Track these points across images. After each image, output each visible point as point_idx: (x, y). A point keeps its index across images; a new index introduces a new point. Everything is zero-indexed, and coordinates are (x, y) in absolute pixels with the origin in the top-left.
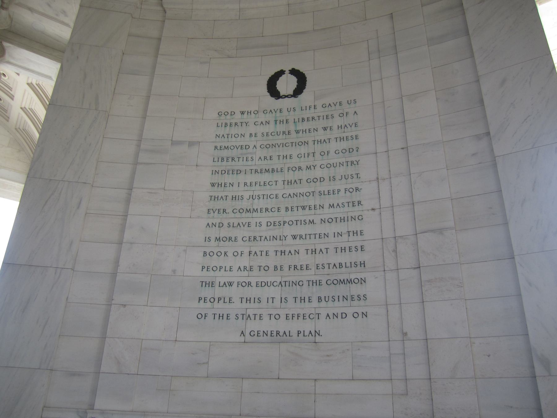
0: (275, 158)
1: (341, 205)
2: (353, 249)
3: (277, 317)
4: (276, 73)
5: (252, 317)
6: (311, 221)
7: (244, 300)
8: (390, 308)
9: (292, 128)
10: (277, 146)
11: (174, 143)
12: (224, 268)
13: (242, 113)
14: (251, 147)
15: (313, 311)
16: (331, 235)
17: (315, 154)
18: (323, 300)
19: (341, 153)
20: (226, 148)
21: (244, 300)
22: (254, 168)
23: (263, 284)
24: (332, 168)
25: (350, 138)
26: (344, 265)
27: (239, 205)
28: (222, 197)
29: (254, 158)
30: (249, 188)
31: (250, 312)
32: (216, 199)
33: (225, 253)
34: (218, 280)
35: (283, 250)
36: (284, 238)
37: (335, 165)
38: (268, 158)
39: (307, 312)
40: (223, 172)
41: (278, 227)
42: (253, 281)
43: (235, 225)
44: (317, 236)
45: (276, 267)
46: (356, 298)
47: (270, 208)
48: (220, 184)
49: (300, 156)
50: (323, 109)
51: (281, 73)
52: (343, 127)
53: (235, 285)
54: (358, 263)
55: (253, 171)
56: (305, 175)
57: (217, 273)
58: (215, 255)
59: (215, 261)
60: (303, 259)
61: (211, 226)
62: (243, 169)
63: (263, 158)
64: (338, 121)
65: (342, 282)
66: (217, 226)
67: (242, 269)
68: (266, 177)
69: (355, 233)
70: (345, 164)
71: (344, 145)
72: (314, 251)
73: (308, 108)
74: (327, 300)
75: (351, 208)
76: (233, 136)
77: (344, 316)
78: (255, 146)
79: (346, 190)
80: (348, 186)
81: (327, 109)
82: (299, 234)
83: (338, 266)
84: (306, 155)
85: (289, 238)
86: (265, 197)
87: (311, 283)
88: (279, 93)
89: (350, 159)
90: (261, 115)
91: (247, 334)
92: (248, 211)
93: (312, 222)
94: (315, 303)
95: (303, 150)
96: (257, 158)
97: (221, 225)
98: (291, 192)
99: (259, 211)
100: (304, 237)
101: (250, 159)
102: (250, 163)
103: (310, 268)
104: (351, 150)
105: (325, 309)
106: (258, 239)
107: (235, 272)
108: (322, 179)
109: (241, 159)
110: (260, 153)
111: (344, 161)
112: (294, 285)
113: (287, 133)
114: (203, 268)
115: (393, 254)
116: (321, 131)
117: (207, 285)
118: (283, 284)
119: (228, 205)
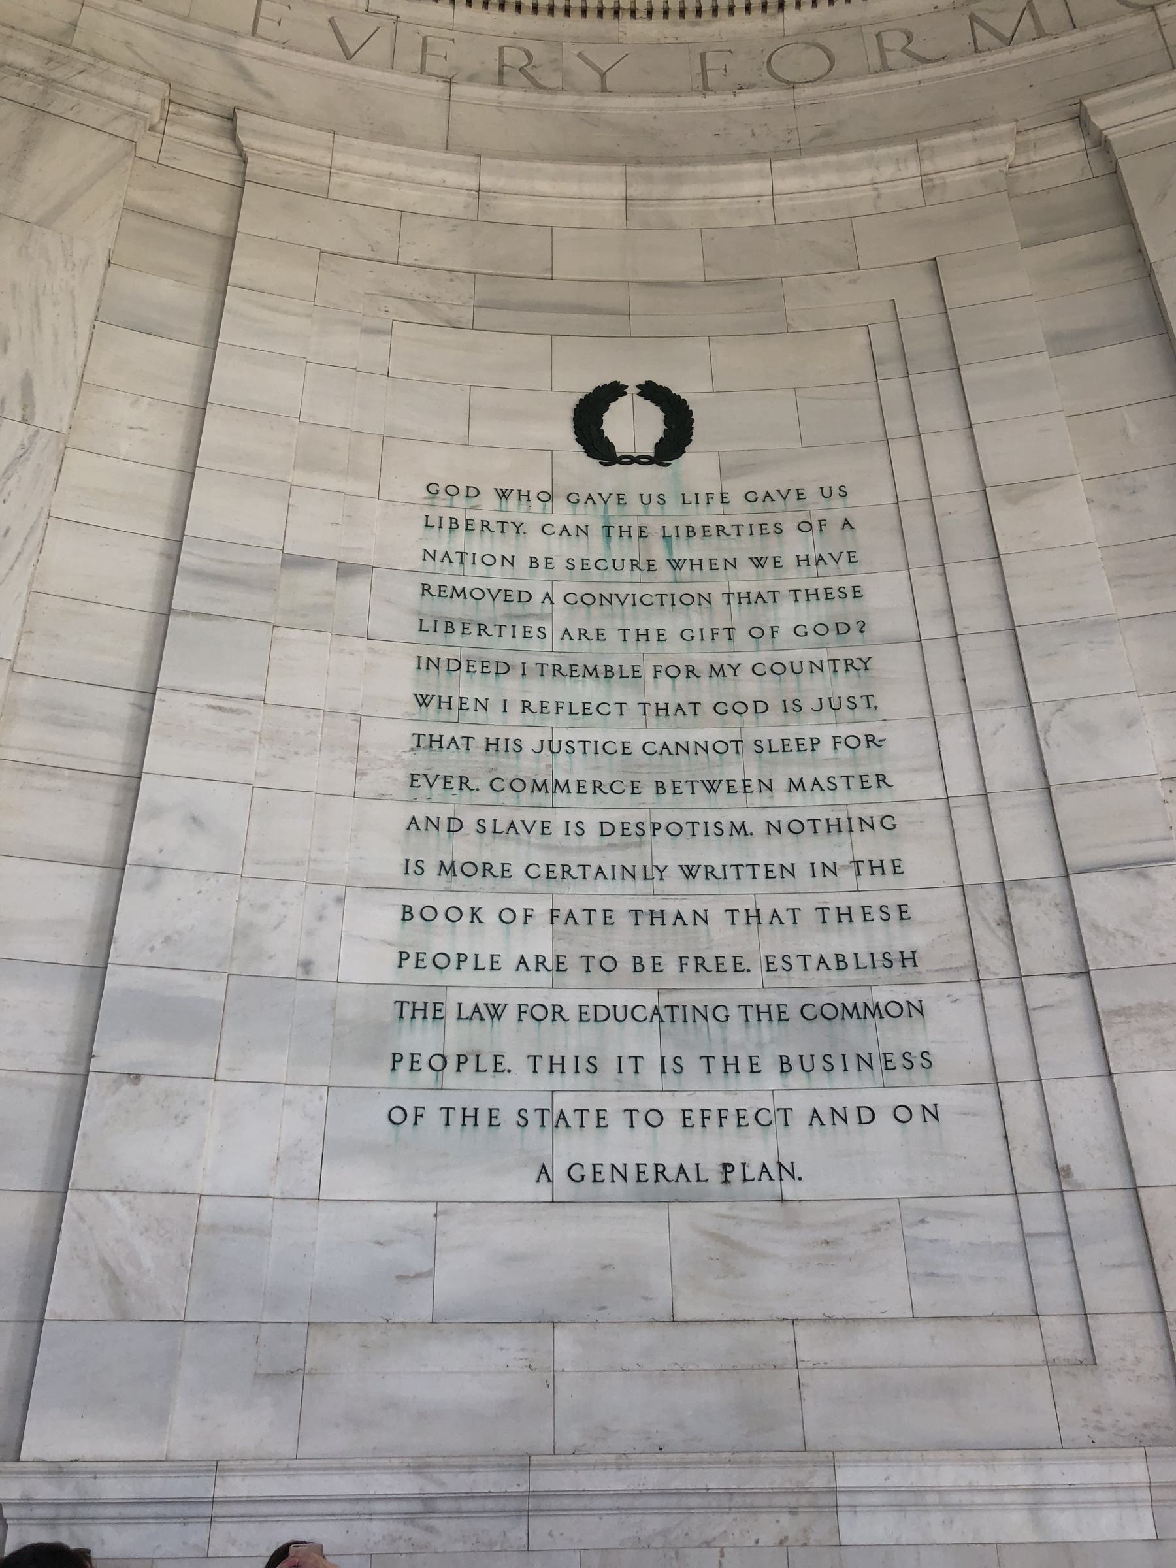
0: (612, 636)
3: (654, 1118)
4: (598, 389)
7: (543, 1065)
8: (1005, 1090)
9: (658, 552)
11: (291, 562)
12: (471, 959)
13: (503, 495)
14: (538, 597)
16: (803, 870)
17: (735, 634)
19: (811, 634)
21: (543, 1065)
22: (550, 660)
23: (602, 1013)
26: (850, 960)
27: (509, 767)
29: (548, 632)
31: (563, 1102)
32: (436, 745)
33: (474, 914)
34: (454, 997)
35: (657, 909)
36: (657, 874)
38: (592, 634)
39: (750, 1103)
40: (454, 665)
41: (635, 839)
42: (570, 1001)
43: (502, 826)
44: (760, 872)
45: (637, 962)
46: (898, 1061)
47: (606, 780)
49: (687, 635)
50: (748, 507)
51: (614, 391)
53: (511, 1013)
54: (895, 956)
55: (548, 670)
56: (706, 691)
57: (451, 976)
58: (441, 917)
60: (722, 938)
62: (516, 660)
63: (575, 634)
64: (794, 545)
65: (851, 1011)
67: (532, 964)
68: (588, 690)
69: (878, 867)
71: (819, 612)
73: (702, 499)
74: (807, 1066)
75: (857, 795)
77: (867, 1116)
78: (547, 596)
80: (844, 731)
82: (704, 863)
84: (707, 634)
85: (674, 873)
87: (752, 1014)
88: (611, 446)
90: (560, 504)
92: (540, 787)
93: (740, 829)
94: (771, 1077)
95: (696, 619)
97: (455, 826)
99: (573, 787)
100: (719, 872)
101: (534, 632)
102: (535, 644)
104: (843, 629)
107: (507, 975)
109: (507, 632)
110: (561, 617)
111: (825, 659)
112: (699, 1018)
113: (644, 566)
114: (403, 957)
115: (1001, 932)
116: (749, 570)
117: (419, 1015)
119: (475, 762)
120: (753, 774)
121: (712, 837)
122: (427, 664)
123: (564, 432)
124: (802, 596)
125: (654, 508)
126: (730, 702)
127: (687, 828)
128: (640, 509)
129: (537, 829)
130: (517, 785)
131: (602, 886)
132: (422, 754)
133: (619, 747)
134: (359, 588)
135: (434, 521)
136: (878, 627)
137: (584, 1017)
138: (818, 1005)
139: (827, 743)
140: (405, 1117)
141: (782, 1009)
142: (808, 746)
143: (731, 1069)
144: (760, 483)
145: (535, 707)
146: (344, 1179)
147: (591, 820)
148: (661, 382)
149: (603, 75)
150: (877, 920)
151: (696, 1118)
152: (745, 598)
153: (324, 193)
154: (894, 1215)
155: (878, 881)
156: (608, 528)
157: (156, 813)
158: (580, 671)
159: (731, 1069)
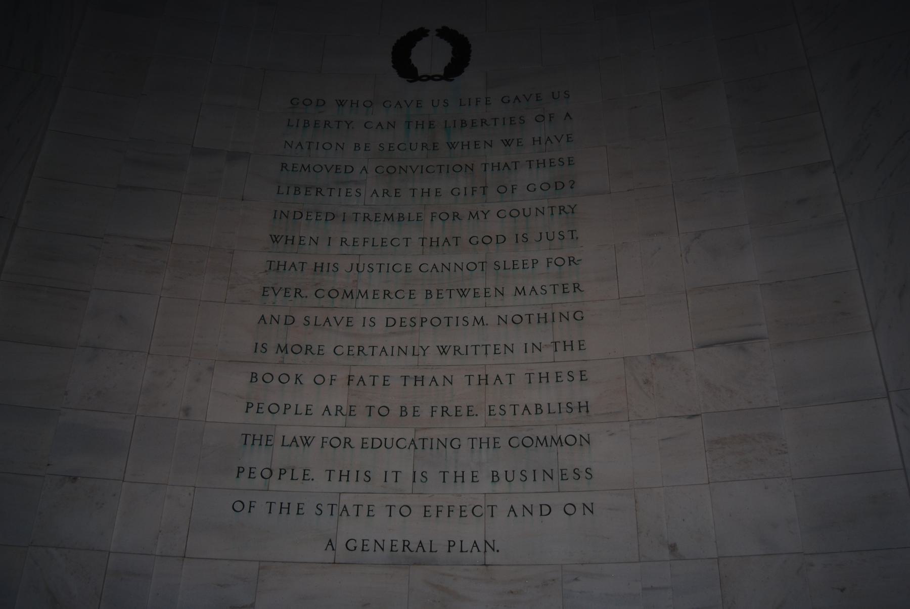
2: (565, 377)
3: (405, 511)
4: (409, 33)
5: (352, 511)
6: (479, 319)
10: (409, 170)
18: (503, 479)
19: (539, 190)
28: (293, 265)
29: (362, 192)
31: (345, 500)
32: (281, 268)
35: (419, 375)
37: (527, 213)
41: (409, 328)
43: (321, 321)
44: (491, 350)
45: (403, 410)
47: (393, 290)
48: (290, 237)
52: (543, 142)
53: (317, 443)
58: (276, 381)
61: (268, 321)
66: (282, 321)
68: (387, 230)
69: (568, 345)
70: (547, 211)
72: (484, 380)
74: (510, 478)
76: (320, 146)
77: (546, 510)
82: (453, 344)
83: (532, 409)
84: (469, 191)
86: (384, 268)
87: (477, 443)
91: (340, 544)
92: (349, 295)
93: (480, 321)
94: (485, 485)
99: (370, 295)
100: (463, 350)
101: (353, 192)
106: (368, 351)
108: (501, 239)
114: (249, 406)
118: (419, 444)
124: (534, 164)
127: (445, 321)
137: (365, 446)
141: (497, 440)
150: (565, 381)
151: (433, 511)
158: (382, 217)
159: (459, 479)
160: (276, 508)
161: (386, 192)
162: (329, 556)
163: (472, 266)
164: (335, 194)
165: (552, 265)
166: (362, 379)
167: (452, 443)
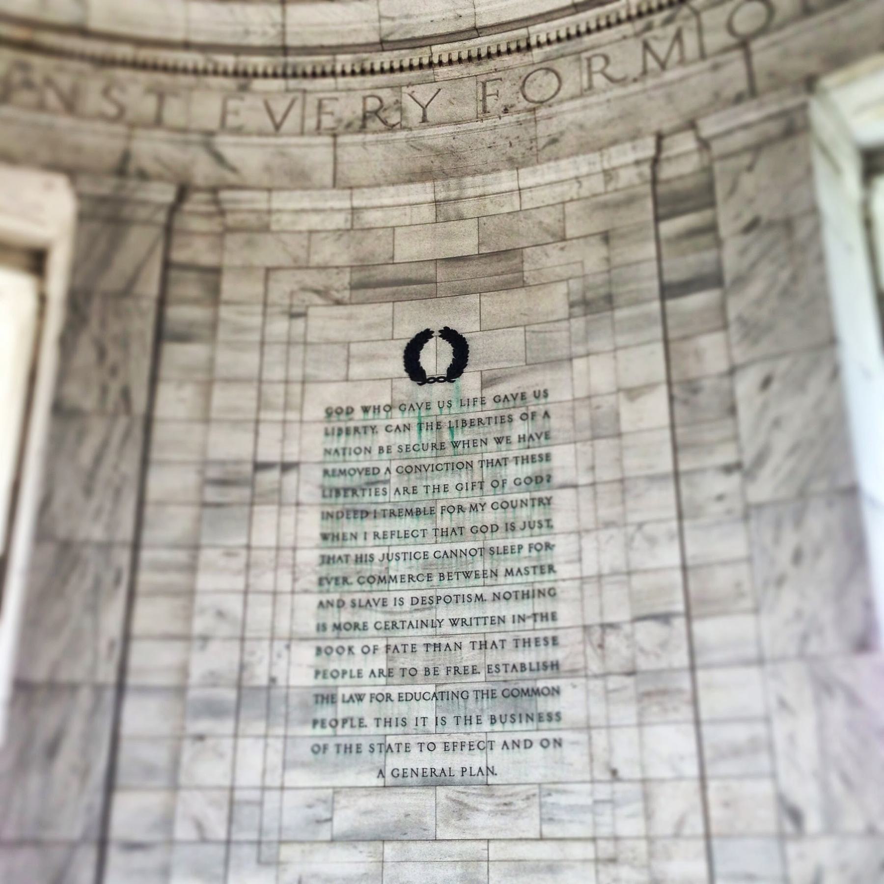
1: (523, 571)
4: (418, 335)
5: (395, 748)
7: (382, 723)
9: (446, 437)
10: (423, 469)
11: (259, 467)
13: (365, 410)
14: (383, 471)
15: (483, 737)
16: (509, 619)
19: (523, 484)
20: (343, 472)
21: (382, 723)
22: (388, 507)
23: (409, 697)
24: (510, 509)
25: (537, 458)
26: (527, 666)
29: (388, 491)
30: (381, 542)
31: (391, 740)
36: (438, 623)
37: (514, 504)
38: (410, 490)
39: (474, 738)
41: (428, 605)
42: (394, 691)
43: (363, 603)
44: (488, 621)
45: (427, 670)
47: (415, 574)
50: (495, 406)
51: (424, 336)
52: (527, 439)
53: (367, 699)
56: (469, 520)
57: (340, 681)
59: (335, 664)
60: (468, 657)
63: (401, 491)
64: (520, 428)
65: (526, 693)
68: (408, 523)
69: (544, 617)
70: (530, 503)
71: (528, 470)
72: (483, 645)
74: (503, 720)
75: (538, 578)
77: (528, 744)
78: (388, 469)
79: (530, 546)
80: (535, 540)
81: (501, 405)
82: (461, 617)
83: (519, 668)
84: (470, 486)
86: (408, 556)
88: (423, 372)
89: (537, 495)
90: (396, 413)
92: (382, 580)
93: (480, 598)
94: (486, 726)
95: (464, 477)
96: (393, 492)
97: (341, 604)
98: (447, 547)
99: (399, 580)
100: (468, 622)
101: (381, 491)
102: (381, 499)
103: (478, 670)
105: (500, 734)
106: (399, 625)
108: (495, 528)
110: (395, 481)
112: (455, 698)
113: (438, 447)
114: (317, 673)
116: (492, 445)
120: (488, 567)
121: (466, 602)
122: (326, 516)
123: (397, 366)
125: (446, 411)
126: (479, 525)
128: (438, 411)
129: (380, 603)
130: (371, 579)
131: (412, 632)
132: (325, 567)
133: (422, 555)
134: (291, 478)
135: (330, 430)
136: (559, 477)
138: (511, 689)
139: (526, 547)
140: (319, 749)
142: (516, 550)
143: (468, 722)
144: (503, 389)
145: (381, 535)
146: (296, 777)
147: (407, 596)
148: (453, 326)
149: (424, 108)
151: (451, 746)
152: (490, 463)
153: (265, 229)
154: (536, 791)
155: (544, 625)
156: (420, 425)
157: (203, 611)
159: (468, 722)
160: (342, 749)
161: (406, 490)
162: (380, 782)
163: (473, 552)
164: (367, 493)
165: (533, 550)
166: (396, 647)
167: (463, 695)
